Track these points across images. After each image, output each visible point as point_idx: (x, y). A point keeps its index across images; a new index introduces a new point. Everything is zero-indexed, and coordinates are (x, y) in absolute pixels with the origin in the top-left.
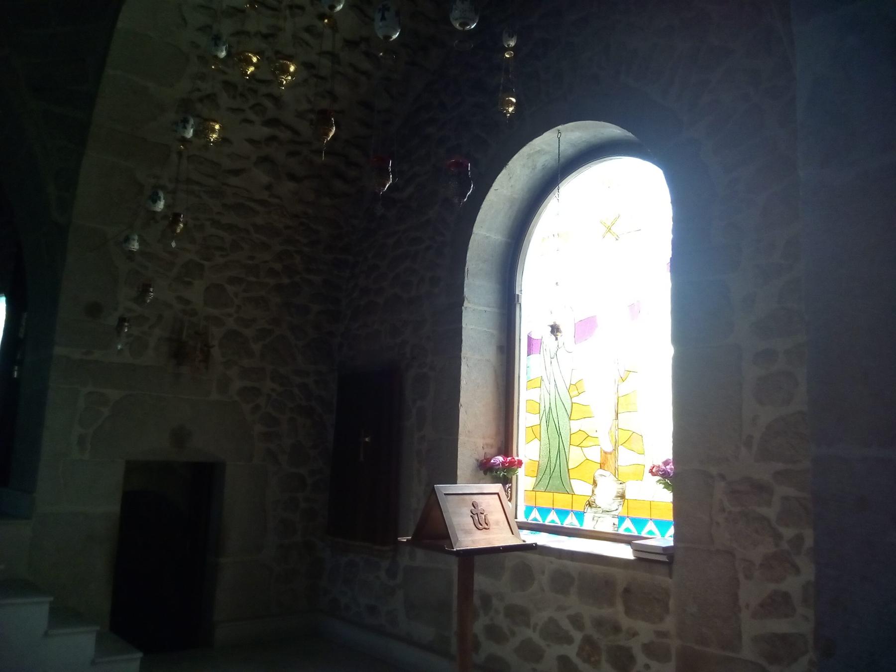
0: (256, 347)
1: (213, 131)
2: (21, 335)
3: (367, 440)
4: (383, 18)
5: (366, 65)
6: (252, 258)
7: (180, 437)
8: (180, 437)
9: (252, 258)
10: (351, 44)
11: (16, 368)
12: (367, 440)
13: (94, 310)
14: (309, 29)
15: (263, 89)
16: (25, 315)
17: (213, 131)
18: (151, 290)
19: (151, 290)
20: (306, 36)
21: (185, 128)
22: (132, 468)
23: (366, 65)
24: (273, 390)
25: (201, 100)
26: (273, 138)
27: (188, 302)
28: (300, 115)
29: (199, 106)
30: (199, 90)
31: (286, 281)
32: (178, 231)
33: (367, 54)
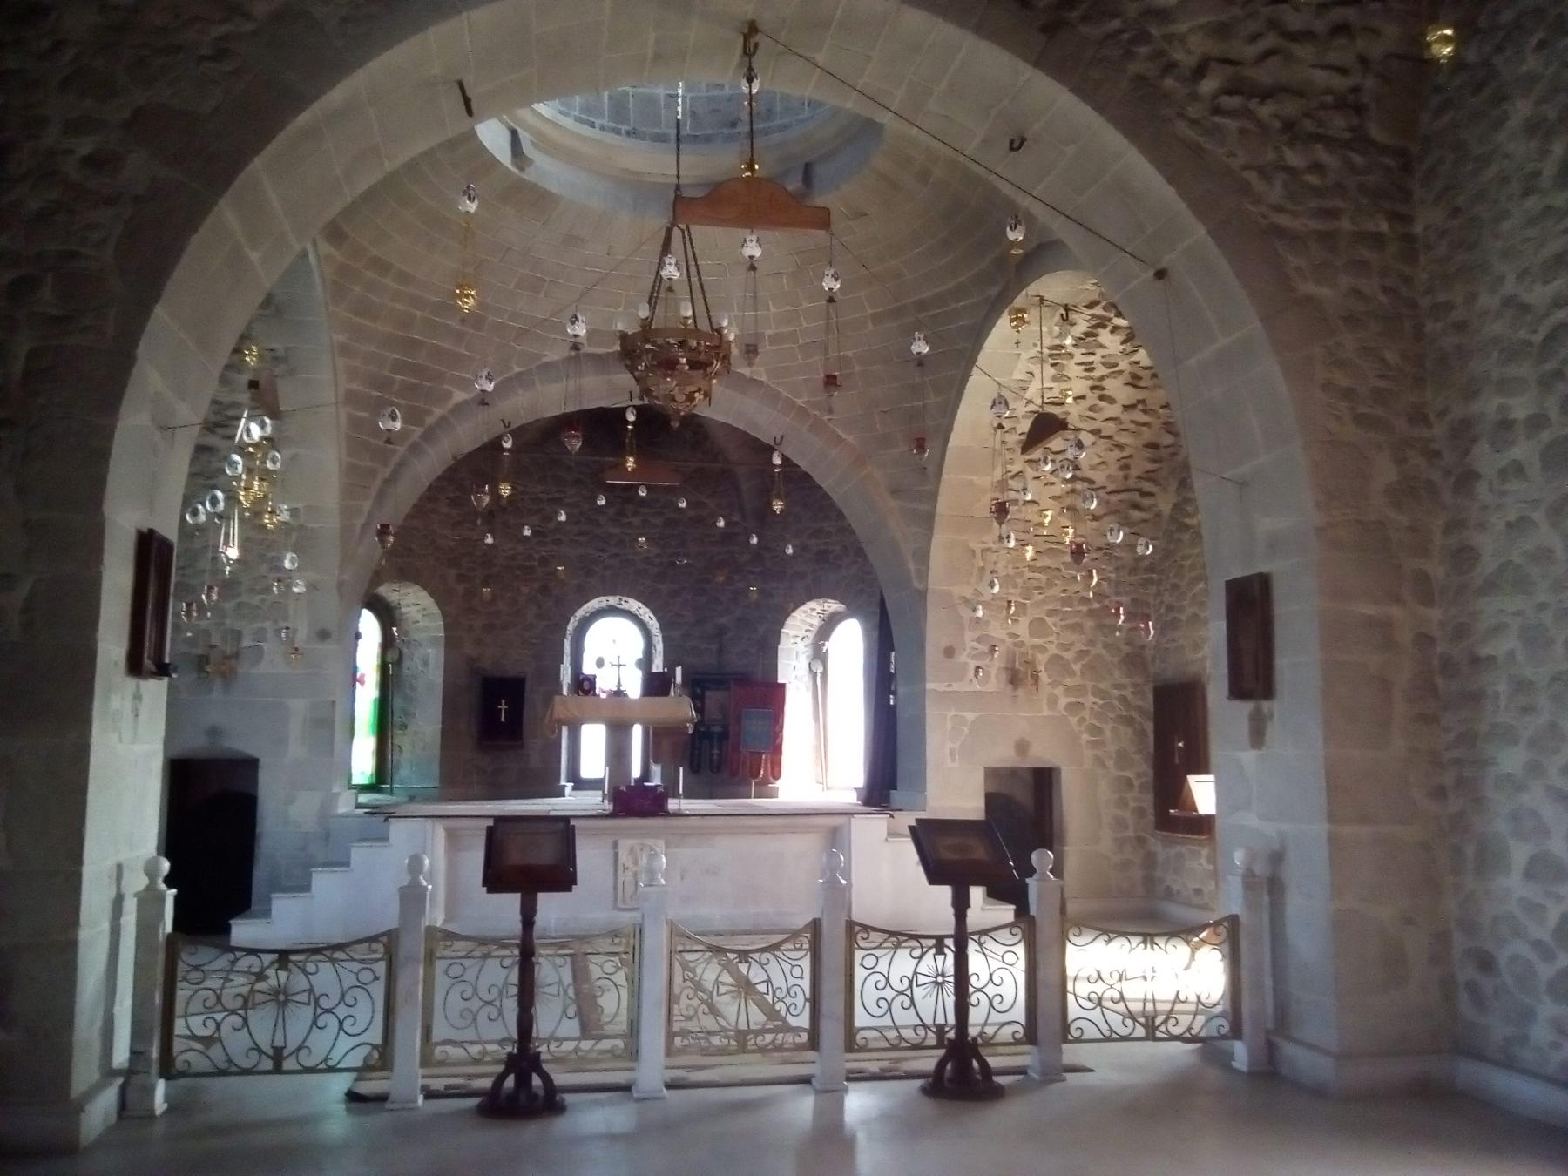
0: (1077, 667)
1: (1028, 551)
2: (893, 671)
3: (1181, 744)
4: (1111, 535)
5: (1144, 418)
6: (1064, 591)
7: (1022, 747)
8: (1022, 747)
9: (1064, 591)
10: (1128, 408)
11: (891, 696)
12: (1181, 744)
13: (949, 652)
14: (1091, 409)
15: (1060, 457)
16: (893, 654)
17: (1028, 551)
18: (997, 649)
19: (997, 649)
20: (1091, 414)
21: (1008, 542)
22: (992, 774)
23: (1144, 418)
24: (1094, 703)
25: (1013, 477)
26: (1073, 491)
27: (1017, 636)
28: (1092, 468)
29: (1010, 482)
30: (1010, 472)
31: (1096, 605)
32: (1012, 612)
33: (1145, 412)
